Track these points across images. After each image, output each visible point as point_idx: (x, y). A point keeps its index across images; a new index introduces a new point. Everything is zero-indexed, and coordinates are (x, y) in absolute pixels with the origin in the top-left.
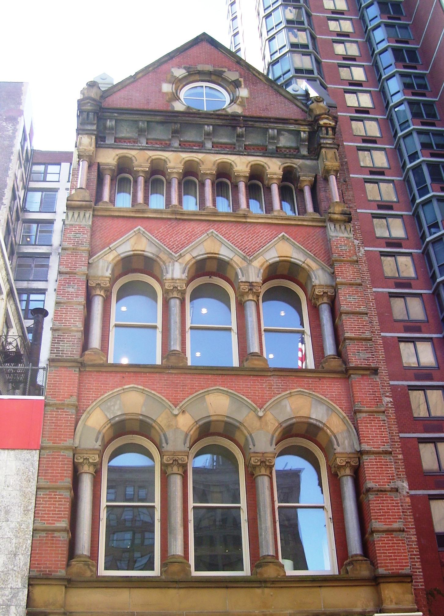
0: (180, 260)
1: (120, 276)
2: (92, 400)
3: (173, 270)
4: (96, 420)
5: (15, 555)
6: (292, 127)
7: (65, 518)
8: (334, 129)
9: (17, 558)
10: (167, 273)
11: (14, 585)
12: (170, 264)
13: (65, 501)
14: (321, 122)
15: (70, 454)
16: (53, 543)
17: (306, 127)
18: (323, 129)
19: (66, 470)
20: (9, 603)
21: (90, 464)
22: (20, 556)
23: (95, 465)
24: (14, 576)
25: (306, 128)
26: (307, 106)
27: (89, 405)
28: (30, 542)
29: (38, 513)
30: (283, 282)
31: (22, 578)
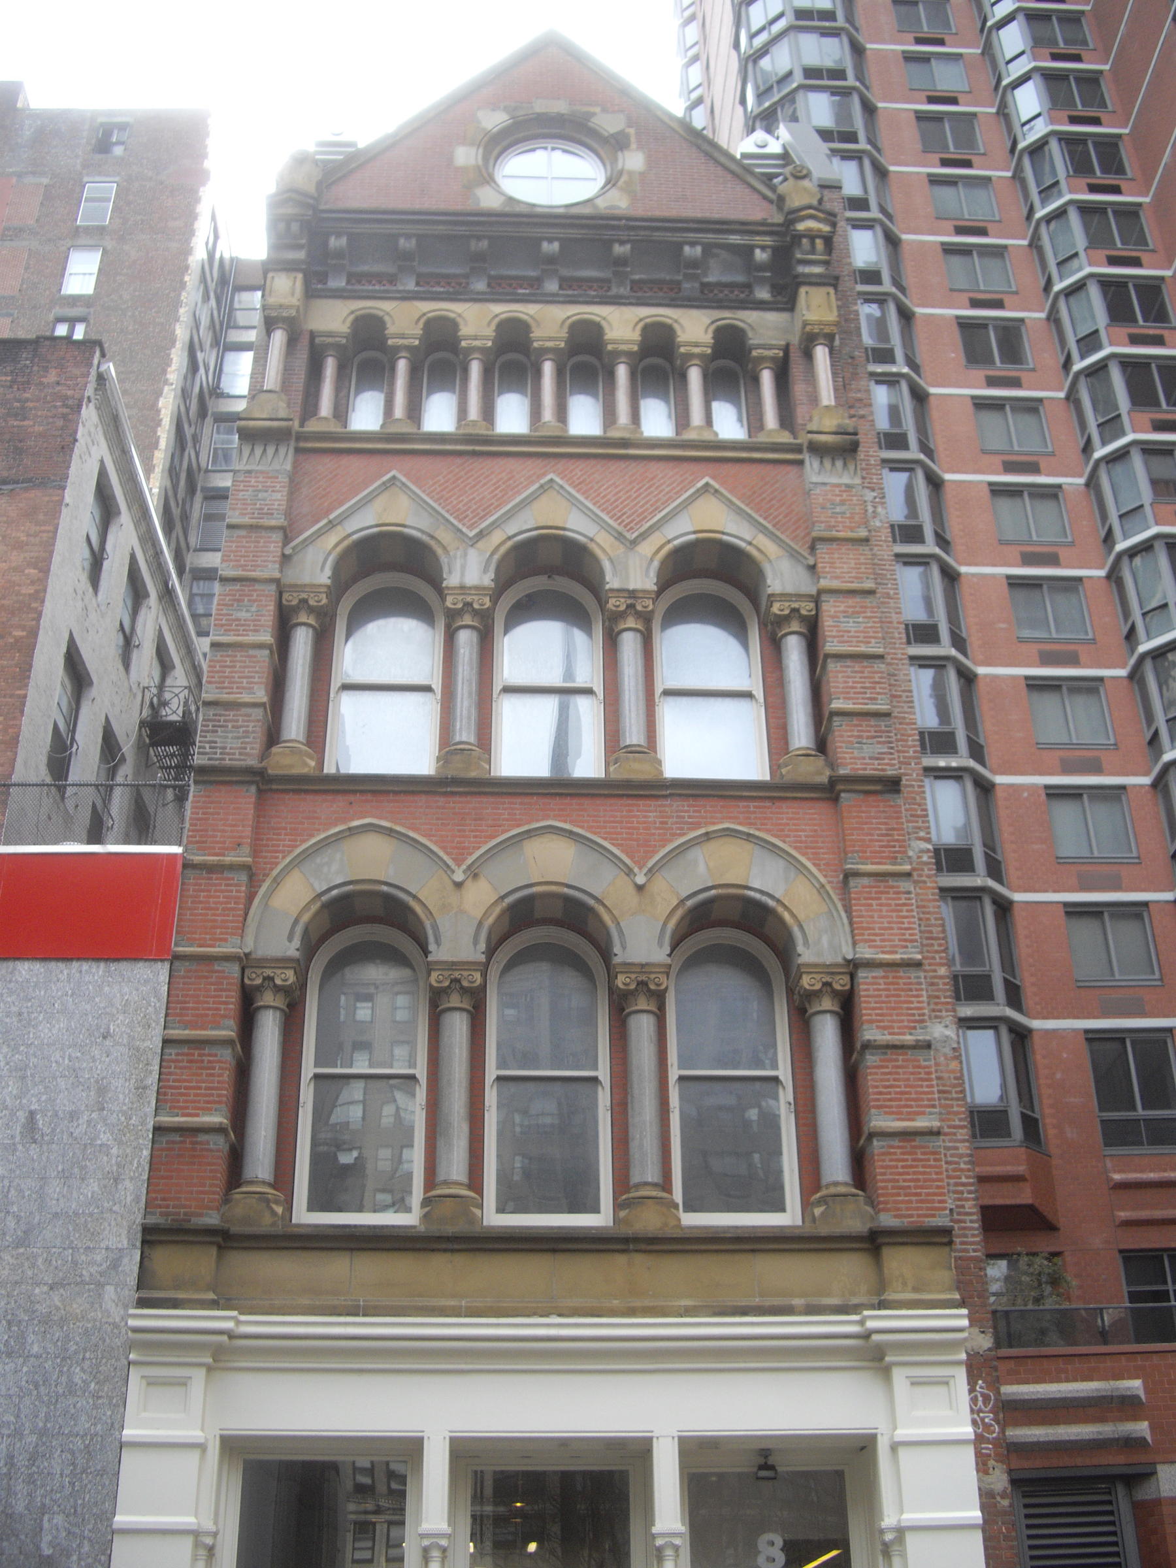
0: (480, 545)
1: (355, 580)
2: (283, 852)
3: (463, 567)
4: (293, 896)
5: (116, 1180)
6: (735, 239)
7: (220, 1102)
8: (828, 240)
9: (120, 1187)
10: (450, 572)
11: (112, 1242)
12: (459, 553)
13: (221, 1068)
14: (801, 226)
15: (234, 970)
16: (194, 1156)
17: (767, 238)
18: (804, 241)
19: (226, 1003)
20: (102, 1279)
21: (278, 989)
22: (127, 1183)
23: (284, 990)
24: (113, 1223)
25: (768, 240)
26: (773, 189)
27: (277, 864)
28: (146, 1153)
29: (165, 1094)
30: (712, 582)
31: (130, 1228)
